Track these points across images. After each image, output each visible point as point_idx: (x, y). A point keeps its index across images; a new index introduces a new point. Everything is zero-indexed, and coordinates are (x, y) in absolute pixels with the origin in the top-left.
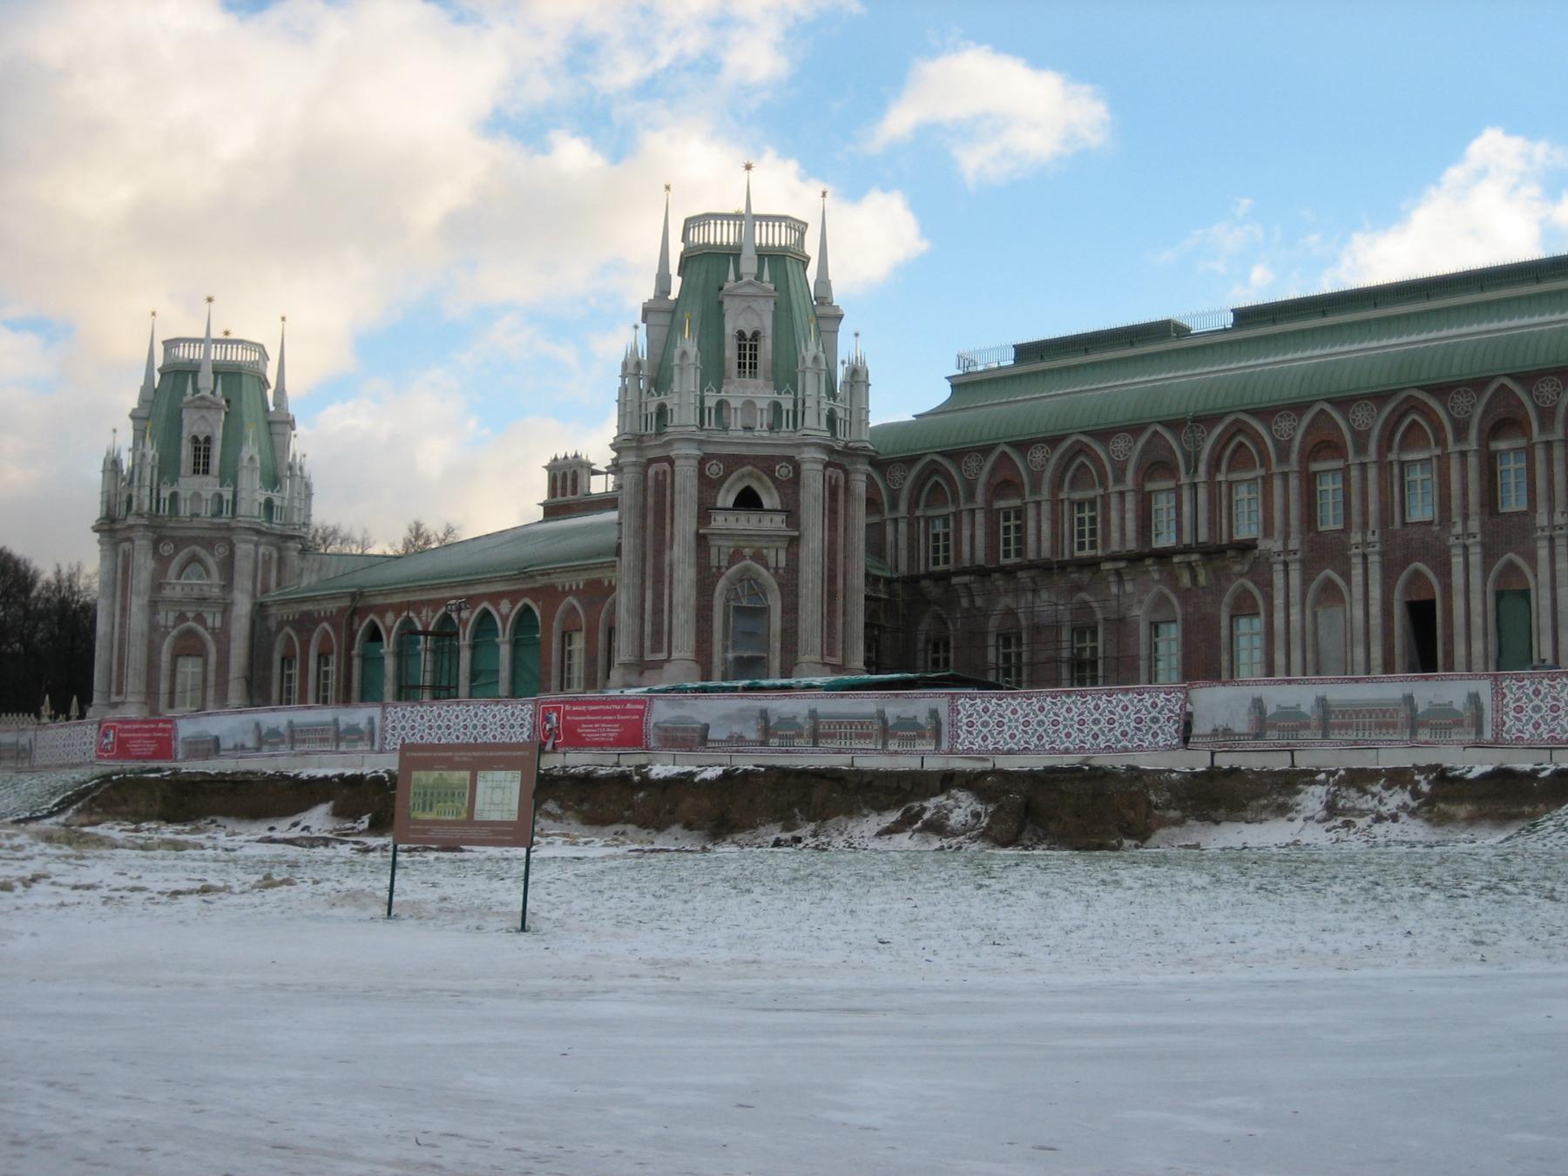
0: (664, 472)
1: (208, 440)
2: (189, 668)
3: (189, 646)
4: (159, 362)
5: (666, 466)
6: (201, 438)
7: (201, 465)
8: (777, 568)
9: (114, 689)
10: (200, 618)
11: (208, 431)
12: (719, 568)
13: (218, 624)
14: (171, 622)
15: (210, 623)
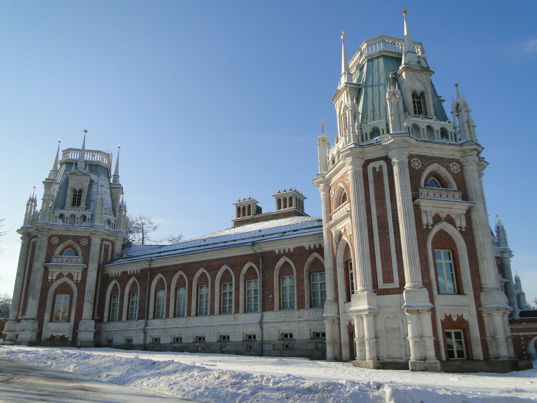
0: (381, 167)
1: (81, 191)
2: (63, 300)
3: (64, 289)
4: (60, 158)
5: (383, 163)
6: (77, 190)
7: (76, 202)
8: (460, 227)
9: (20, 313)
10: (70, 276)
11: (80, 187)
12: (427, 225)
13: (79, 279)
14: (54, 278)
15: (75, 278)
